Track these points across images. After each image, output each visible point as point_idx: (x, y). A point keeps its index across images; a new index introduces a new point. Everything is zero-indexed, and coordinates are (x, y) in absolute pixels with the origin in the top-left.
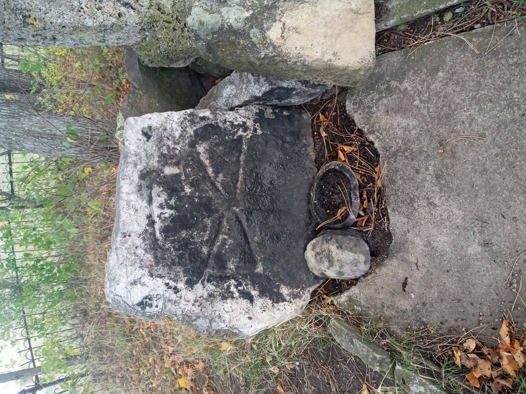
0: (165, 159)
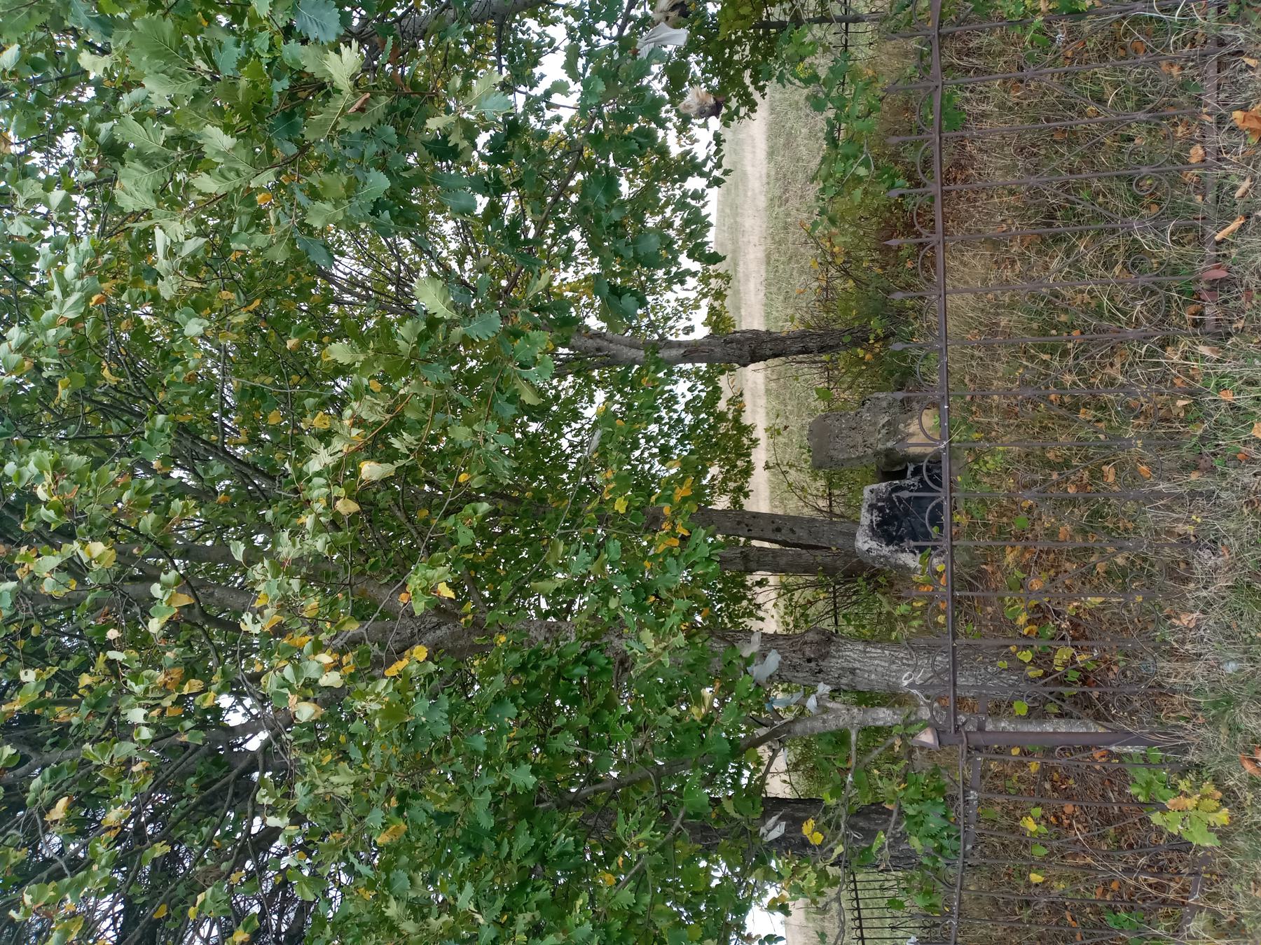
0: (878, 500)
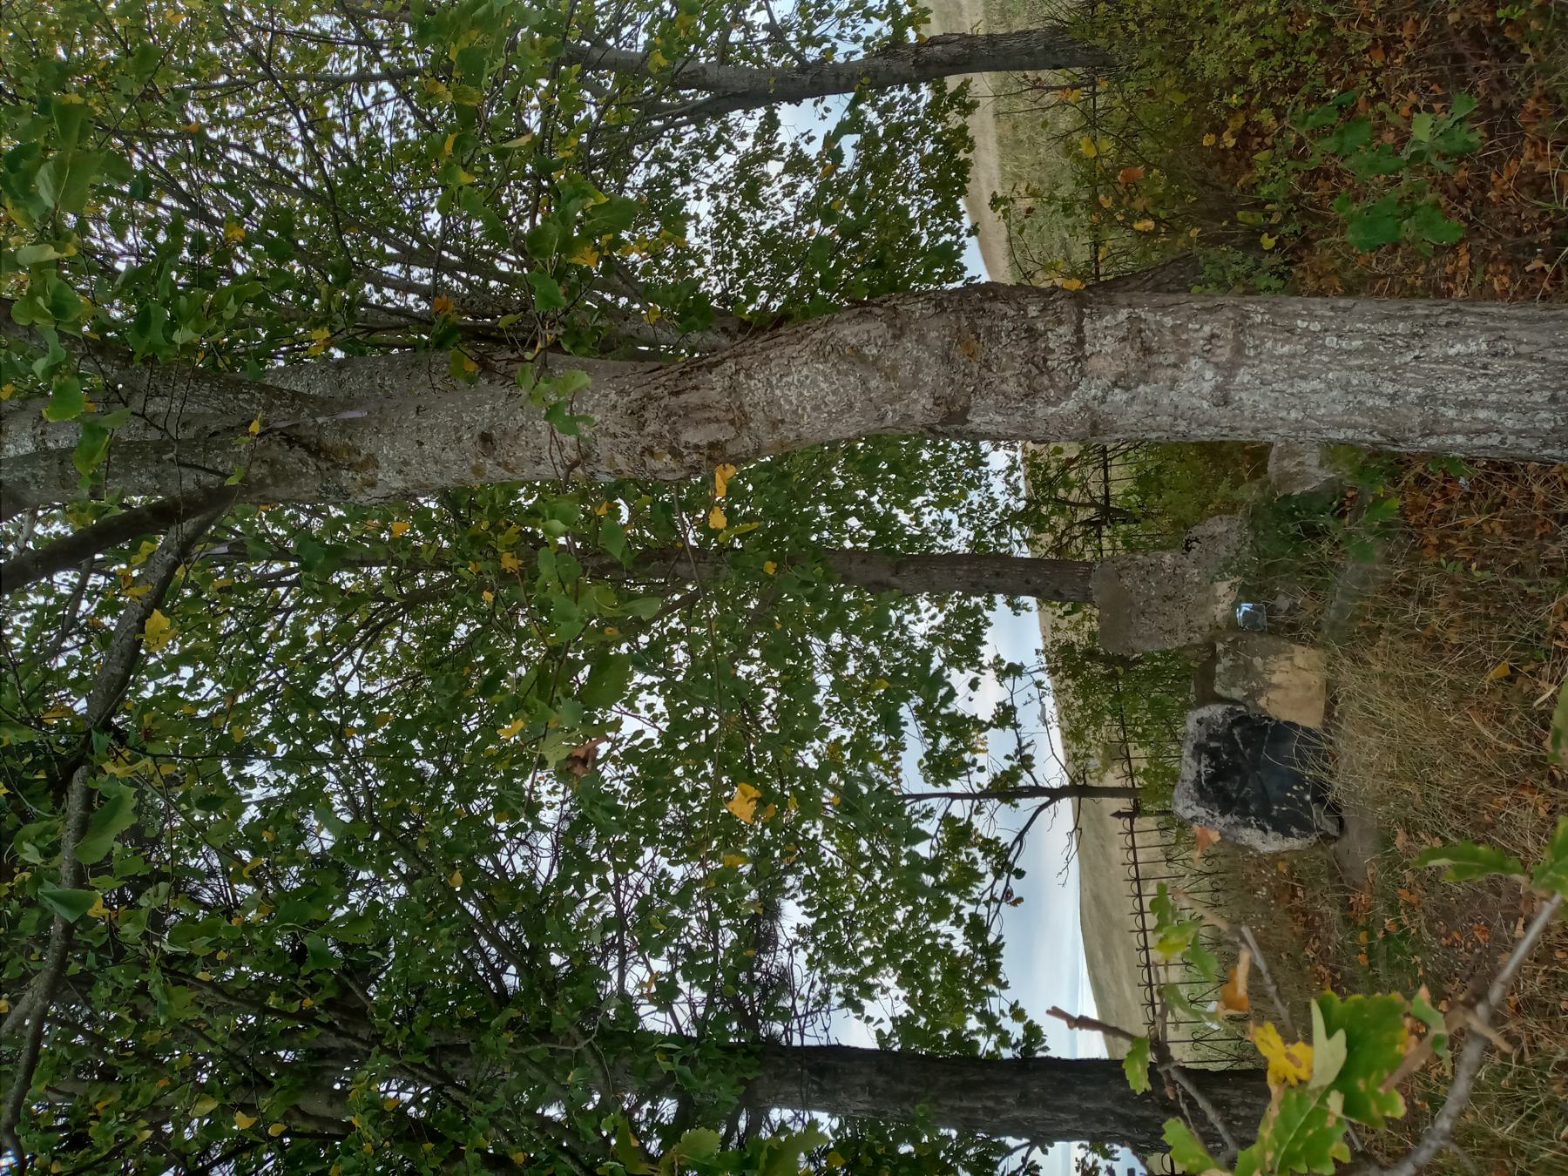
0: (1211, 737)
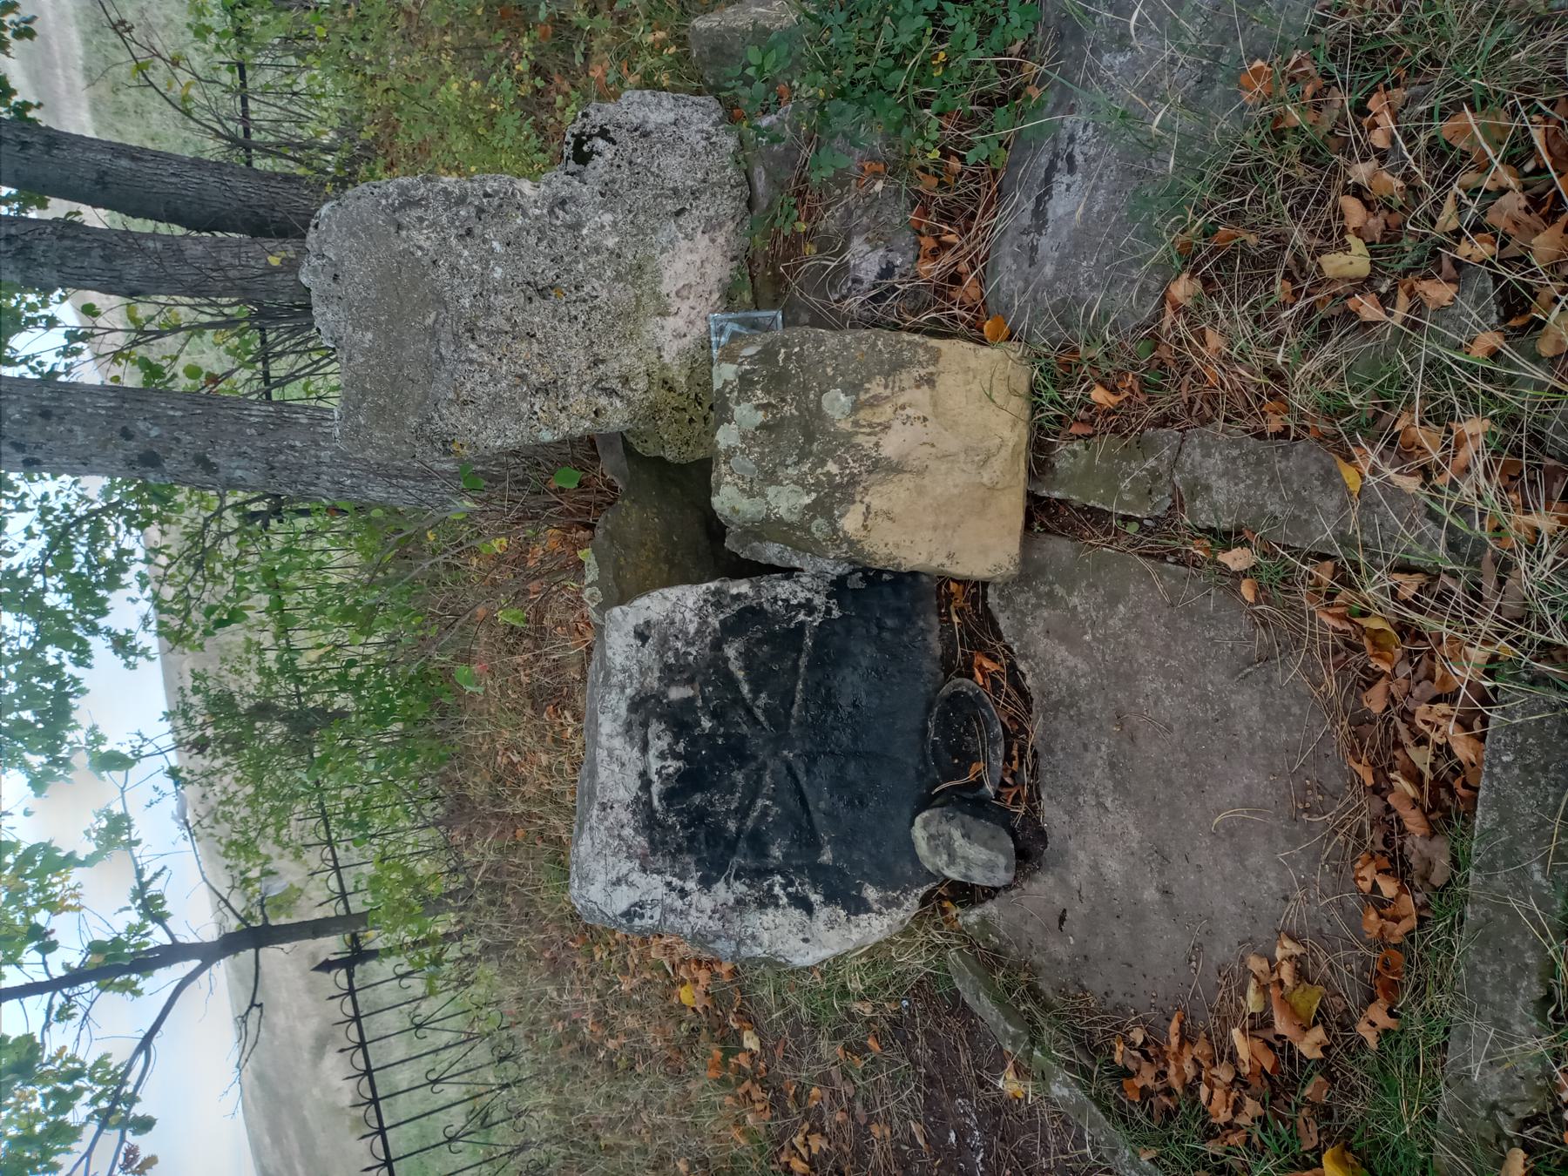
0: (670, 674)
